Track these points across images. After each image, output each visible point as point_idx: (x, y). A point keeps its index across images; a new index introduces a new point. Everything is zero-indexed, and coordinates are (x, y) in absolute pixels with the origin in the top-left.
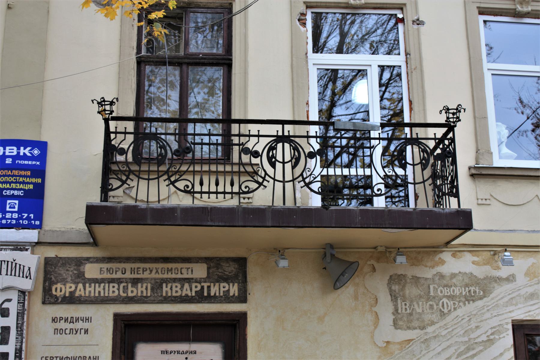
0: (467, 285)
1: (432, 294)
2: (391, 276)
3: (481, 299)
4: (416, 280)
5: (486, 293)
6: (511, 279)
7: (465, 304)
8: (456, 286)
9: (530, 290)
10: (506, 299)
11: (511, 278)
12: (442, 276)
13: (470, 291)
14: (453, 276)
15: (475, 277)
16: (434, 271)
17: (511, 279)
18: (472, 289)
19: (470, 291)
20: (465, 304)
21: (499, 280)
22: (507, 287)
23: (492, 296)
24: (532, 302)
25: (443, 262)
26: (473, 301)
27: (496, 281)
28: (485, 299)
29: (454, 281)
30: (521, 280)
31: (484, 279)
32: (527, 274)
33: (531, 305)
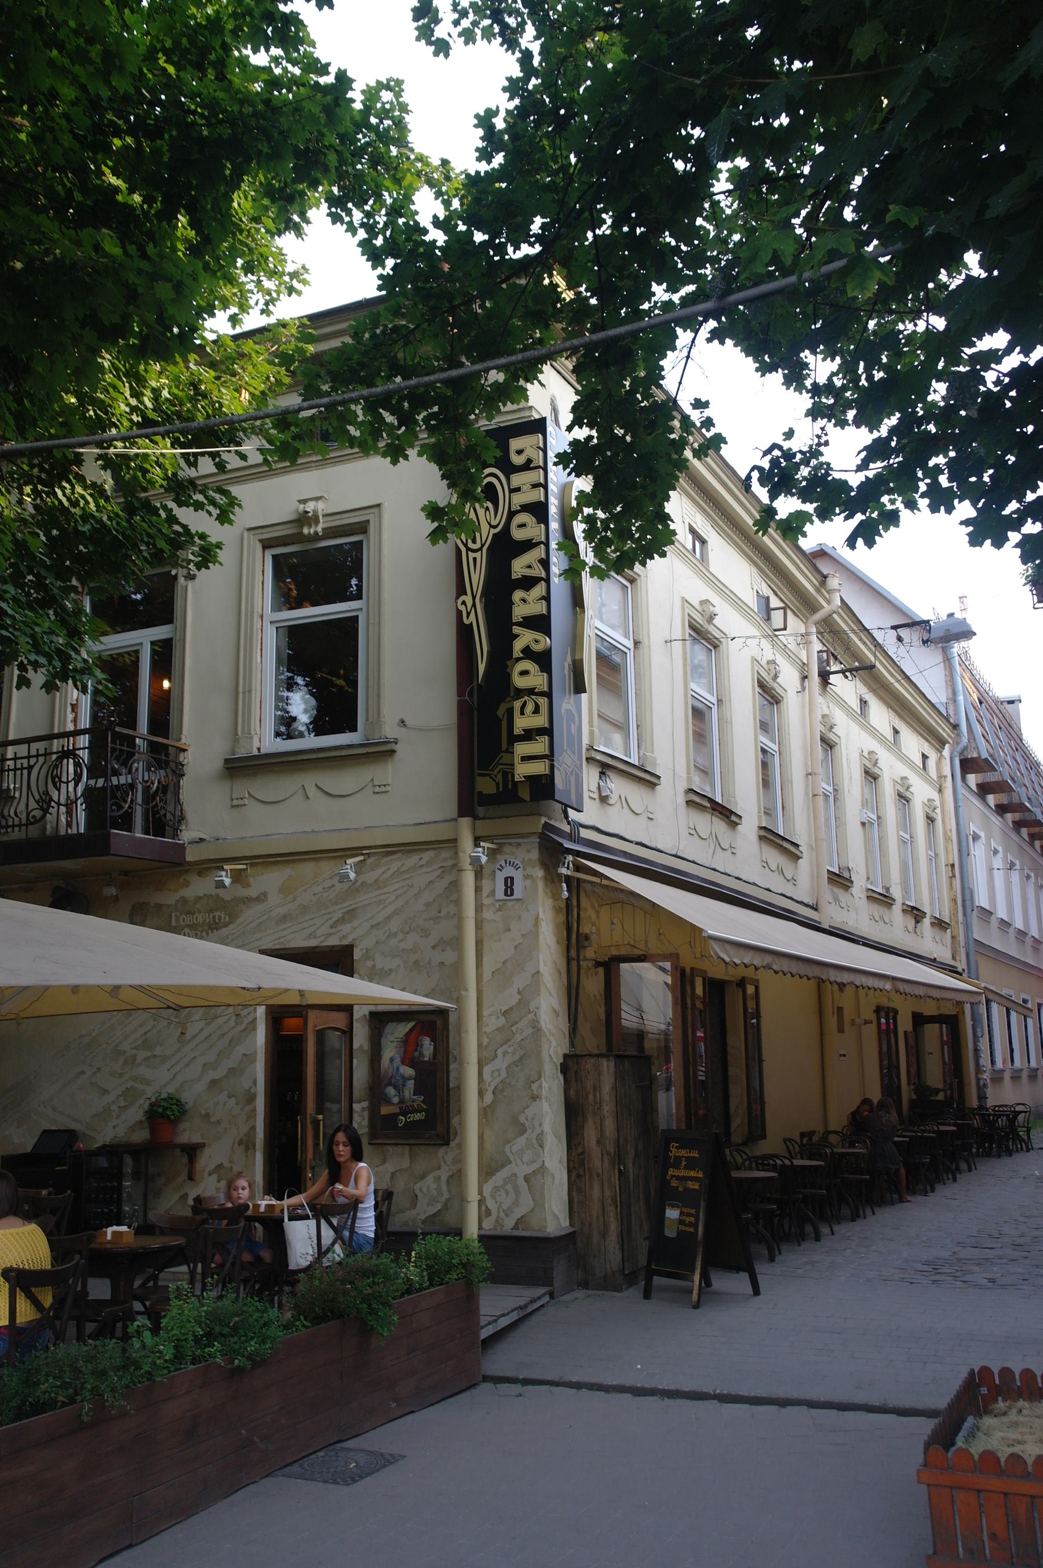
0: (211, 911)
1: (173, 923)
2: (133, 906)
3: (226, 926)
4: (159, 906)
5: (233, 917)
6: (261, 898)
7: (207, 934)
8: (199, 912)
9: (282, 910)
10: (254, 925)
11: (262, 897)
12: (184, 900)
13: (214, 917)
14: (198, 899)
15: (222, 899)
16: (176, 896)
17: (261, 898)
18: (217, 914)
19: (214, 917)
20: (207, 934)
21: (248, 901)
22: (256, 909)
23: (238, 921)
24: (284, 926)
25: (187, 884)
26: (217, 929)
27: (244, 903)
28: (231, 926)
29: (198, 906)
30: (274, 899)
31: (232, 900)
32: (280, 891)
33: (283, 930)
